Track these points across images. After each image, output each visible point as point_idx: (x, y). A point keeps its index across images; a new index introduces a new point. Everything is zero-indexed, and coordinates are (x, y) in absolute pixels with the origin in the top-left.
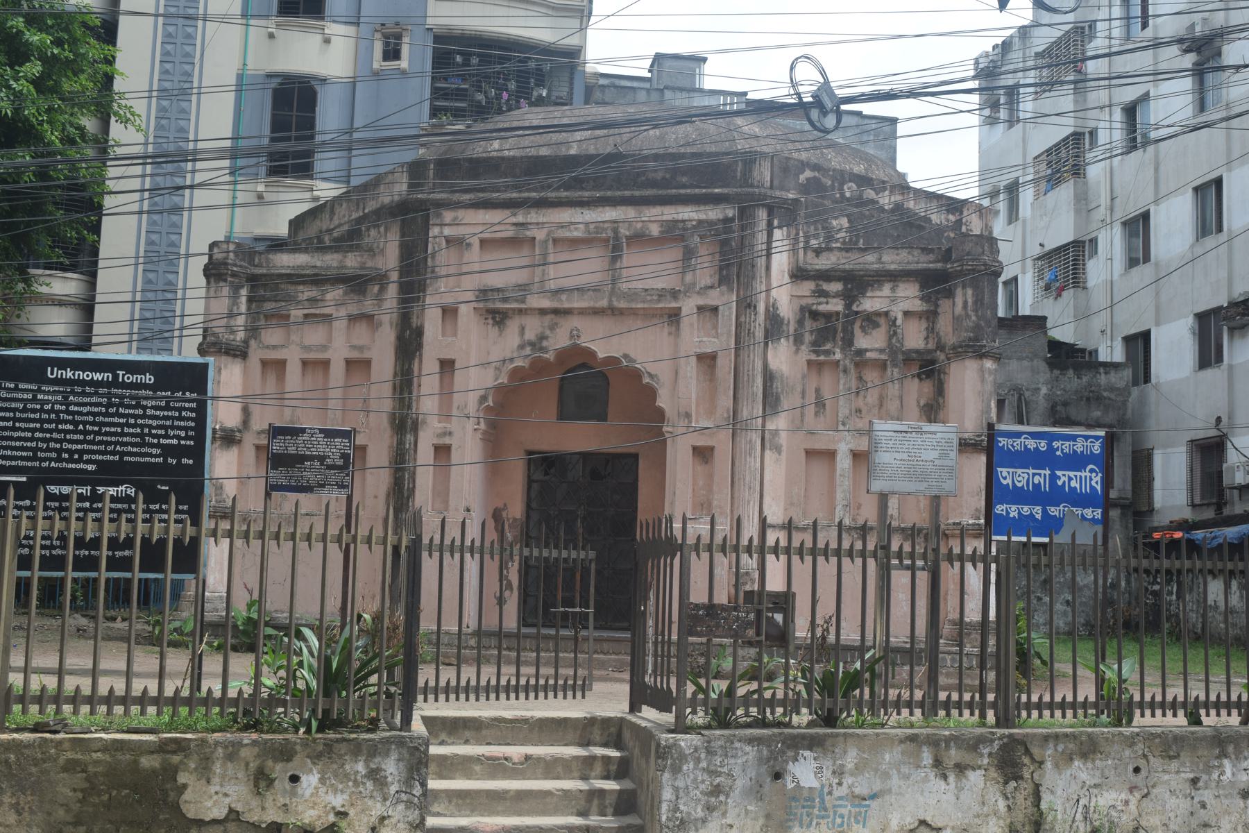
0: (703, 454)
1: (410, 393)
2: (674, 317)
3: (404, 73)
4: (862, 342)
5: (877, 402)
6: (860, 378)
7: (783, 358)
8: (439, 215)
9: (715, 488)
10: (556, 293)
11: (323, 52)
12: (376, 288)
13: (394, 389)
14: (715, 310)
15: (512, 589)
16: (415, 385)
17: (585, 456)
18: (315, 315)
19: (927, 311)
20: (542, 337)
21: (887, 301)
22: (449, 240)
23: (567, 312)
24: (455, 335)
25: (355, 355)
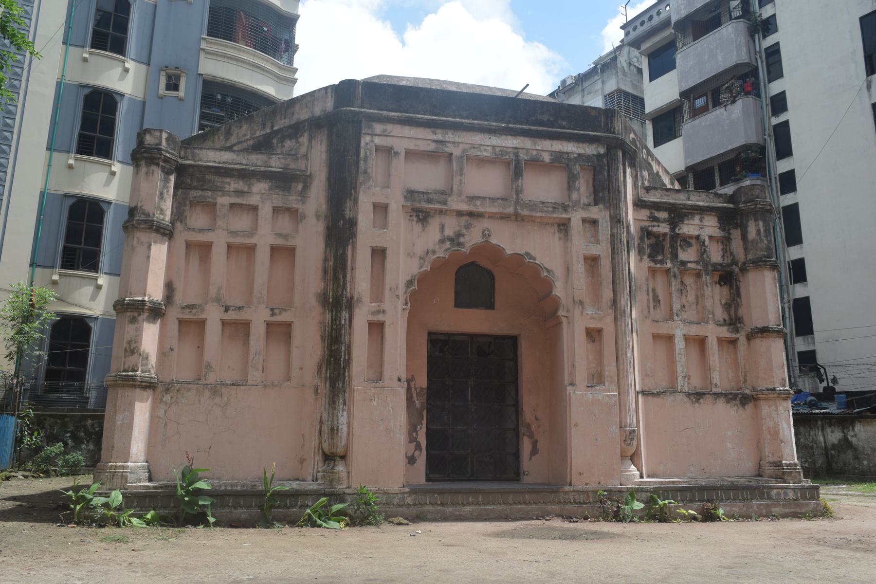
0: (594, 335)
1: (345, 277)
2: (564, 227)
3: (181, 100)
4: (683, 256)
5: (694, 300)
6: (682, 282)
7: (634, 264)
8: (370, 127)
9: (605, 362)
10: (472, 199)
11: (123, 77)
12: (300, 186)
13: (325, 271)
14: (594, 222)
15: (421, 450)
16: (349, 268)
17: (473, 336)
18: (241, 206)
19: (724, 237)
20: (459, 235)
21: (697, 228)
22: (378, 149)
23: (479, 215)
24: (385, 226)
25: (280, 242)
